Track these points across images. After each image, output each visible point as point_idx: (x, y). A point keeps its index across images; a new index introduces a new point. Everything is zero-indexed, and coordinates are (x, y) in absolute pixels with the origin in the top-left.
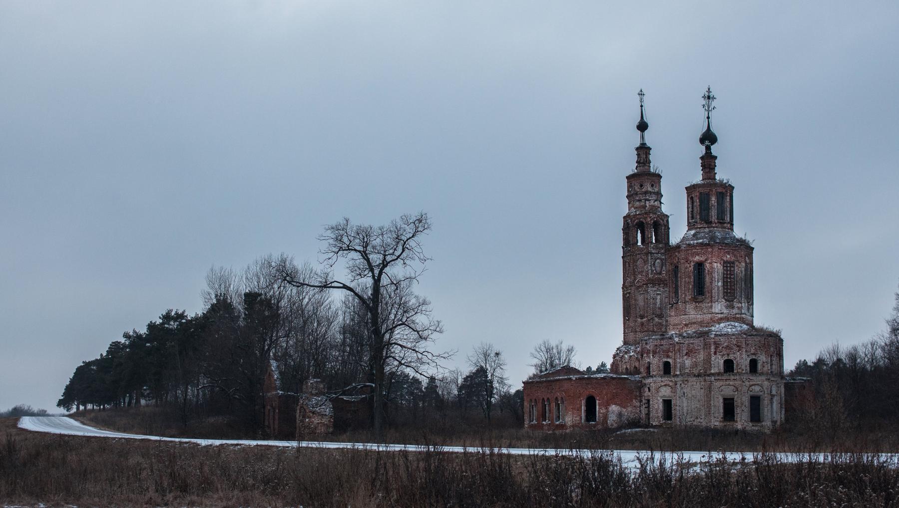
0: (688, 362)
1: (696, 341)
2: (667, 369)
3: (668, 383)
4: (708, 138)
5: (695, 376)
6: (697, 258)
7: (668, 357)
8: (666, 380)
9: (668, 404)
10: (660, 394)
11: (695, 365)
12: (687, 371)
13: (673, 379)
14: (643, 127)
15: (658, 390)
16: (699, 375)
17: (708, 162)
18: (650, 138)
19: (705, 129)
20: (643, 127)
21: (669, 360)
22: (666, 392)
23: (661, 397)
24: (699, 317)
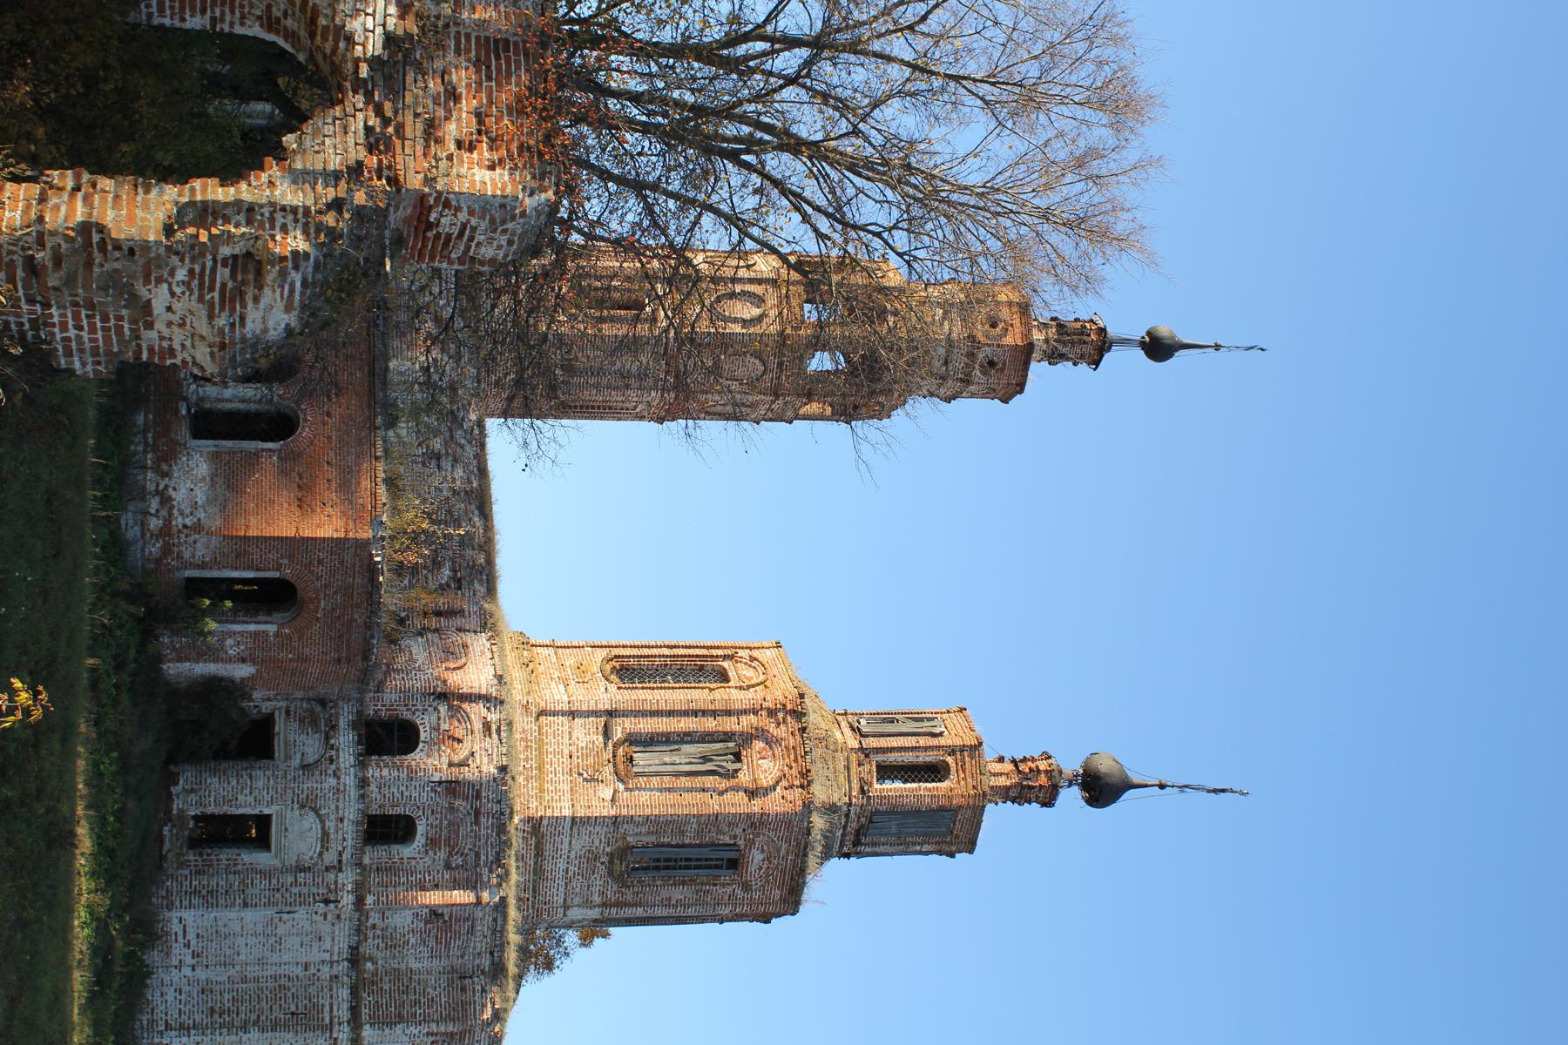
0: (402, 920)
1: (480, 943)
2: (386, 829)
3: (334, 847)
4: (1101, 789)
5: (354, 949)
6: (756, 857)
7: (432, 843)
8: (348, 834)
9: (256, 831)
10: (292, 815)
11: (393, 943)
12: (374, 918)
13: (348, 878)
14: (1158, 348)
15: (309, 804)
16: (355, 959)
17: (1034, 787)
18: (1125, 362)
19: (1136, 779)
20: (1158, 348)
21: (420, 840)
22: (298, 836)
23: (282, 816)
24: (557, 866)
